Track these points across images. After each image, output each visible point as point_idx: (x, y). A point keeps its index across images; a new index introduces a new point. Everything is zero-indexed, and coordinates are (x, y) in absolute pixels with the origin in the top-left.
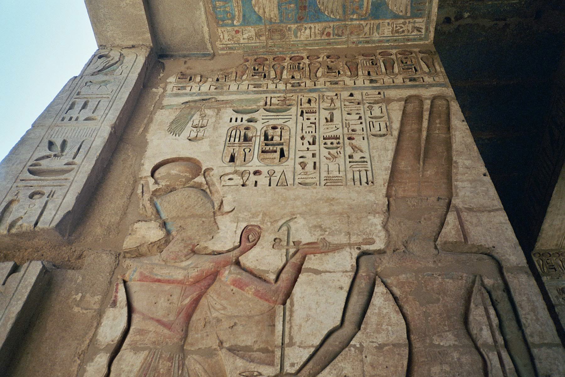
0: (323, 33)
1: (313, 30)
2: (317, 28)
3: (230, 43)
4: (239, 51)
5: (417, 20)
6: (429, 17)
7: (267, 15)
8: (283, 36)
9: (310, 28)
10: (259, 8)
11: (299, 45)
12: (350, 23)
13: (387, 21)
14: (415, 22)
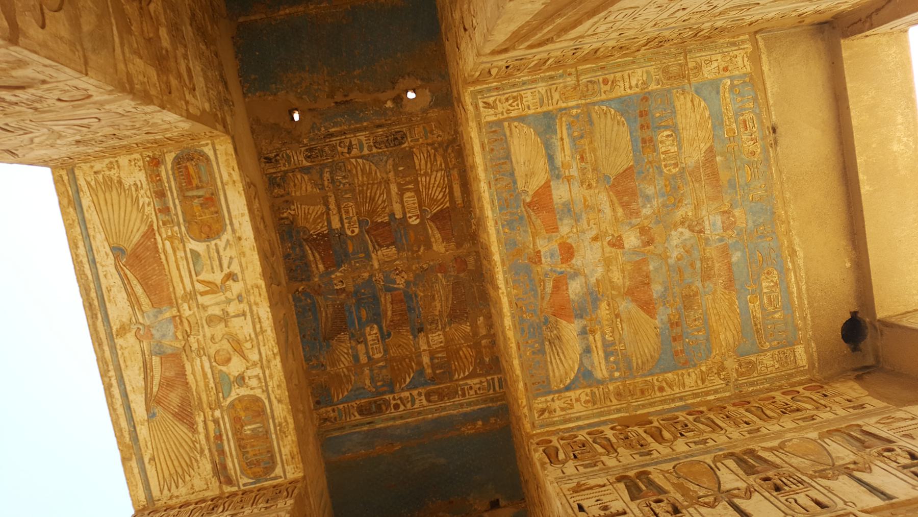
0: (613, 82)
1: (627, 85)
2: (622, 88)
3: (735, 52)
4: (722, 41)
5: (493, 118)
6: (479, 124)
7: (689, 99)
8: (665, 71)
9: (631, 87)
10: (699, 105)
11: (642, 60)
12: (580, 102)
13: (531, 112)
14: (496, 115)
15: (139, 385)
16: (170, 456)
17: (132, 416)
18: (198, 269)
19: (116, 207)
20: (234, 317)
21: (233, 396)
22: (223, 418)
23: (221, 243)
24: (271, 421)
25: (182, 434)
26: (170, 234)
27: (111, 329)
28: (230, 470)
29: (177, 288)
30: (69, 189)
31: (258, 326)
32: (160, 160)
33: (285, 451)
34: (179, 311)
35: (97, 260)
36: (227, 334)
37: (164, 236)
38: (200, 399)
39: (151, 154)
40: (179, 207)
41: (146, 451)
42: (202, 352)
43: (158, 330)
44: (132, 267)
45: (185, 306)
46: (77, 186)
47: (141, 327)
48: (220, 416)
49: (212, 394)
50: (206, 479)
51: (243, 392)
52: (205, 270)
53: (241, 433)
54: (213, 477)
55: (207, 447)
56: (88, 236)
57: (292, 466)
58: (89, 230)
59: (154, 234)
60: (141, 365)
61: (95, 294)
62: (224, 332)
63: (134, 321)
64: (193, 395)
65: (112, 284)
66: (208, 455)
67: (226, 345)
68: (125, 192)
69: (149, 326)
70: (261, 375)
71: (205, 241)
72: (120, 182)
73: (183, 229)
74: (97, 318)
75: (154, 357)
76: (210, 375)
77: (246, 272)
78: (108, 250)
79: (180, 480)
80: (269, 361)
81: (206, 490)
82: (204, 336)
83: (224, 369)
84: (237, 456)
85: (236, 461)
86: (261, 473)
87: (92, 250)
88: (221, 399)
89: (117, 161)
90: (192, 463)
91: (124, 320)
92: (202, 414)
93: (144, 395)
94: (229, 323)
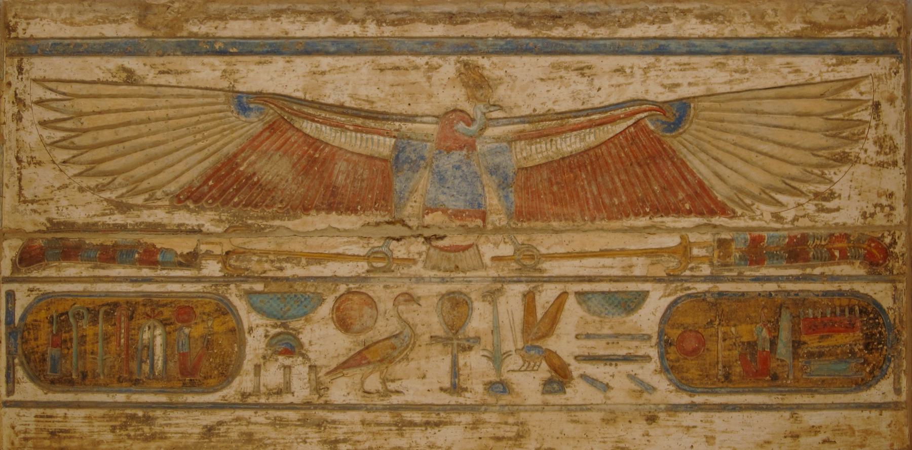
15: (328, 90)
16: (128, 124)
17: (251, 53)
18: (594, 303)
19: (783, 136)
20: (455, 364)
21: (249, 318)
22: (198, 280)
23: (648, 372)
24: (163, 398)
25: (180, 167)
26: (696, 251)
27: (486, 54)
28: (59, 269)
29: (554, 238)
30: (849, 33)
31: (417, 417)
32: (881, 269)
33: (76, 419)
34: (497, 230)
35: (663, 59)
36: (414, 335)
37: (693, 237)
38: (260, 231)
39: (897, 250)
40: (756, 287)
41: (153, 66)
42: (380, 265)
43: (458, 168)
44: (631, 138)
45: (507, 250)
46: (853, 53)
47: (474, 128)
48: (205, 272)
49: (267, 266)
50: (47, 201)
51: (255, 344)
52: (589, 318)
53: (149, 316)
54: (50, 220)
55: (130, 221)
56: (728, 53)
57: (32, 427)
58: (740, 57)
59: (701, 214)
60: (379, 107)
61: (579, 34)
62: (420, 330)
63: (495, 115)
64: (274, 218)
65: (597, 83)
66: (109, 220)
67: (385, 327)
68: (817, 166)
69: (472, 147)
70: (287, 399)
71: (661, 333)
72: (844, 159)
73: (702, 287)
74: (520, 25)
75: (390, 142)
76: (315, 270)
77: (564, 416)
78: (684, 92)
79: (59, 135)
80: (320, 425)
81: (20, 194)
82: (420, 279)
83: (325, 310)
84: (91, 295)
85: (78, 287)
86: (33, 343)
87: (691, 53)
88: (246, 286)
89: (895, 164)
90: (94, 175)
91: (501, 92)
92: (220, 230)
93: (300, 95)
94: (439, 347)
